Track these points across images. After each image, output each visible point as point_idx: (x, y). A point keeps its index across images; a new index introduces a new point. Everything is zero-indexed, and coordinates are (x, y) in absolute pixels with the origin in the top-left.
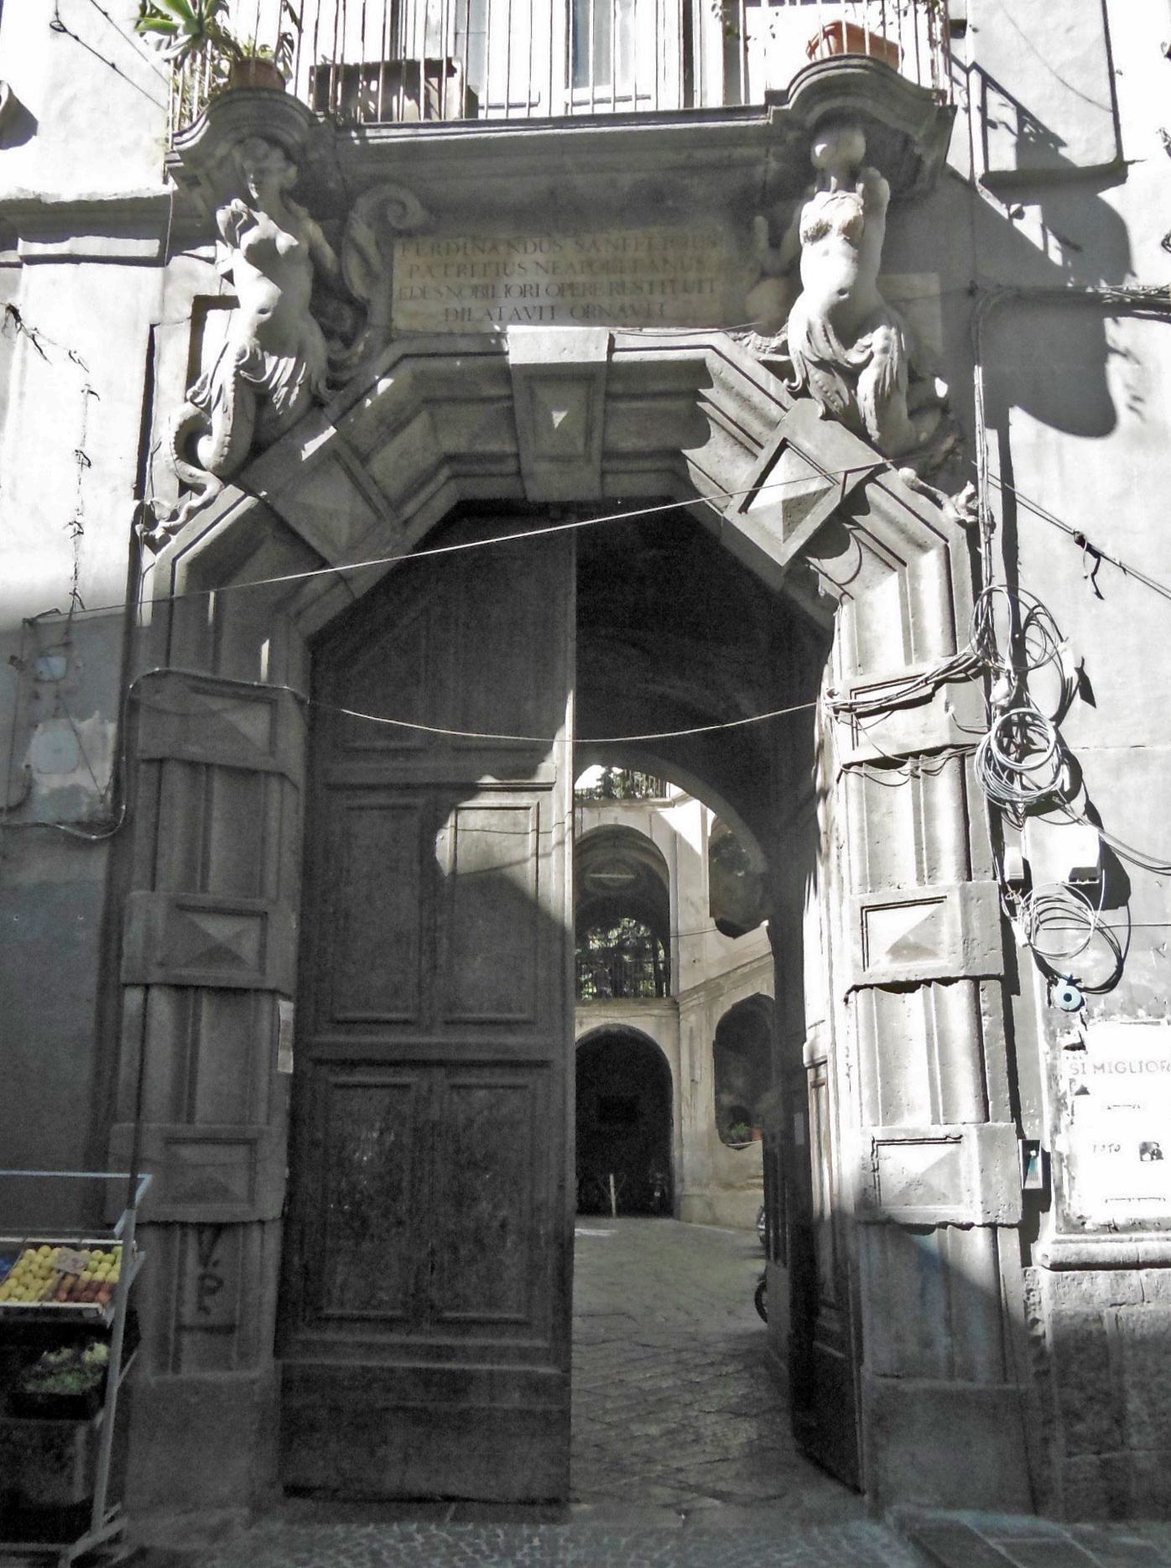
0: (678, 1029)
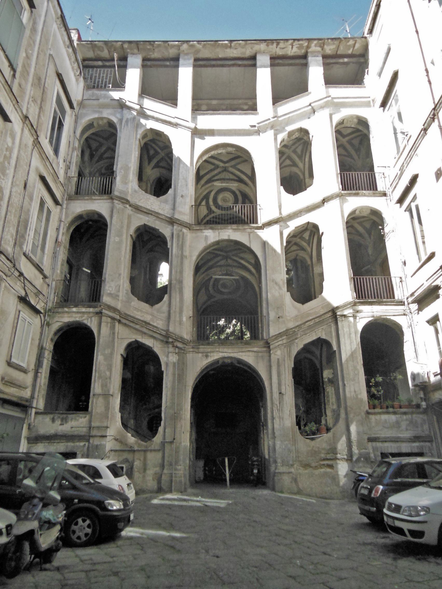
0: (270, 361)
